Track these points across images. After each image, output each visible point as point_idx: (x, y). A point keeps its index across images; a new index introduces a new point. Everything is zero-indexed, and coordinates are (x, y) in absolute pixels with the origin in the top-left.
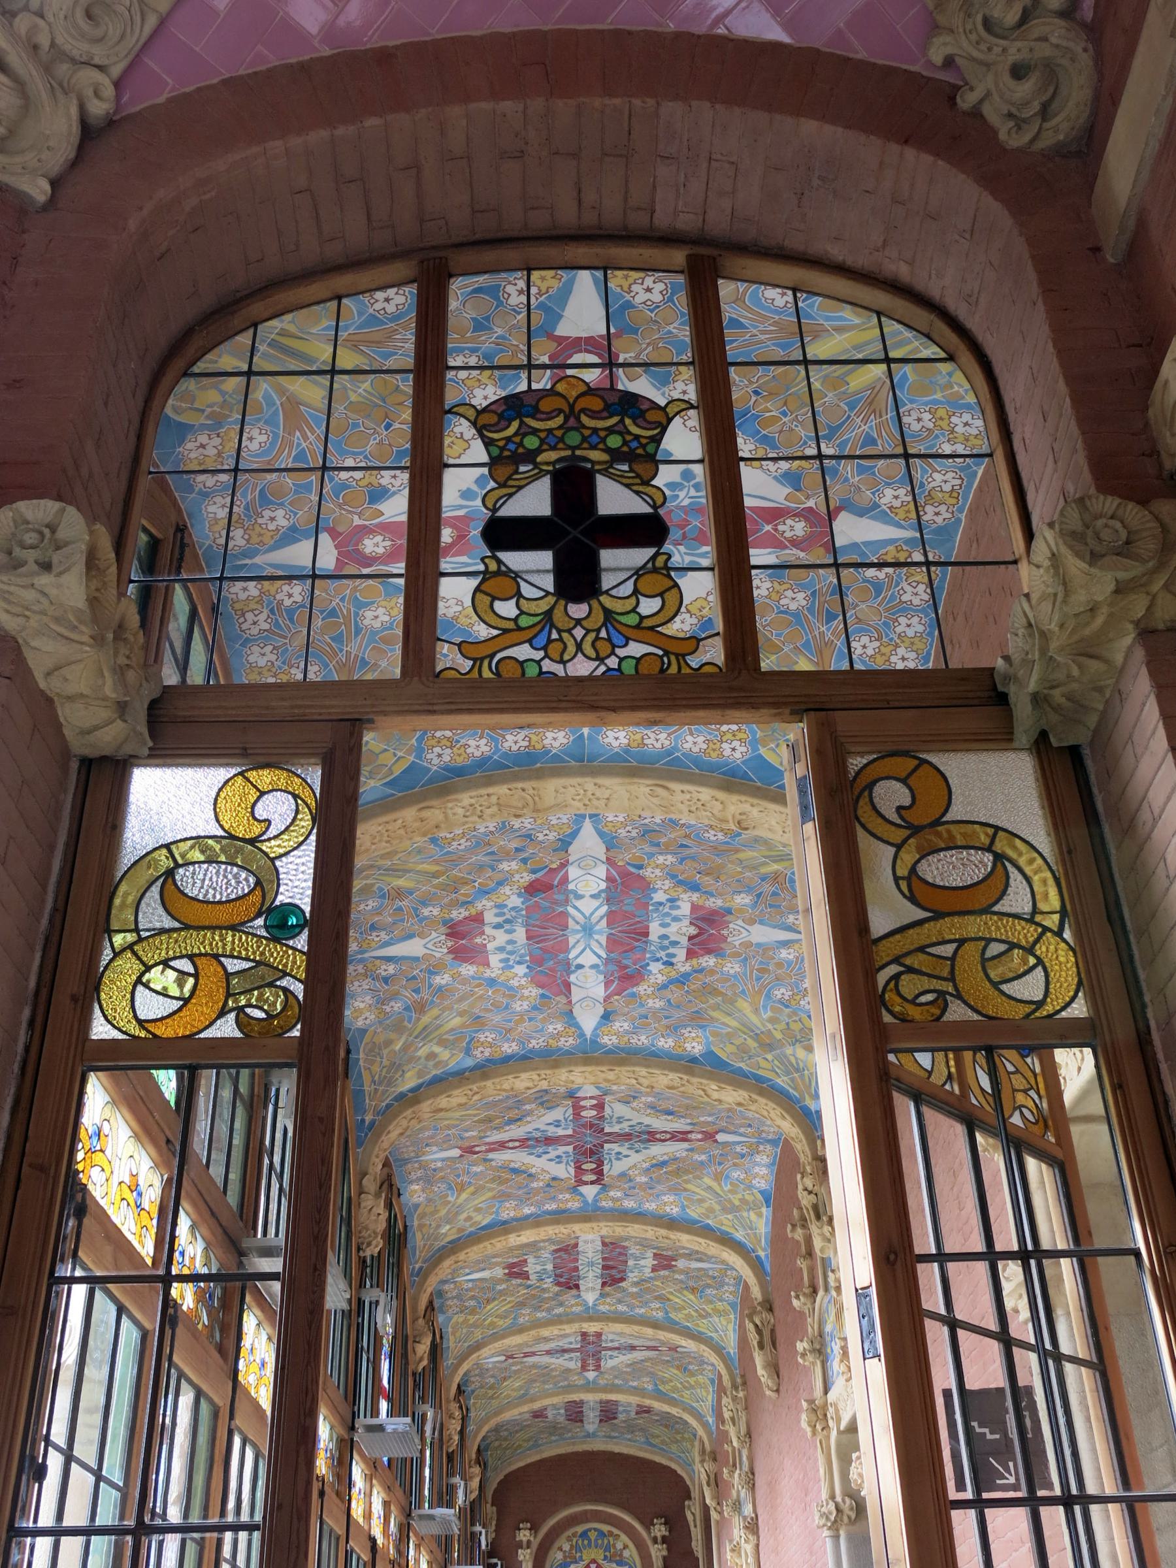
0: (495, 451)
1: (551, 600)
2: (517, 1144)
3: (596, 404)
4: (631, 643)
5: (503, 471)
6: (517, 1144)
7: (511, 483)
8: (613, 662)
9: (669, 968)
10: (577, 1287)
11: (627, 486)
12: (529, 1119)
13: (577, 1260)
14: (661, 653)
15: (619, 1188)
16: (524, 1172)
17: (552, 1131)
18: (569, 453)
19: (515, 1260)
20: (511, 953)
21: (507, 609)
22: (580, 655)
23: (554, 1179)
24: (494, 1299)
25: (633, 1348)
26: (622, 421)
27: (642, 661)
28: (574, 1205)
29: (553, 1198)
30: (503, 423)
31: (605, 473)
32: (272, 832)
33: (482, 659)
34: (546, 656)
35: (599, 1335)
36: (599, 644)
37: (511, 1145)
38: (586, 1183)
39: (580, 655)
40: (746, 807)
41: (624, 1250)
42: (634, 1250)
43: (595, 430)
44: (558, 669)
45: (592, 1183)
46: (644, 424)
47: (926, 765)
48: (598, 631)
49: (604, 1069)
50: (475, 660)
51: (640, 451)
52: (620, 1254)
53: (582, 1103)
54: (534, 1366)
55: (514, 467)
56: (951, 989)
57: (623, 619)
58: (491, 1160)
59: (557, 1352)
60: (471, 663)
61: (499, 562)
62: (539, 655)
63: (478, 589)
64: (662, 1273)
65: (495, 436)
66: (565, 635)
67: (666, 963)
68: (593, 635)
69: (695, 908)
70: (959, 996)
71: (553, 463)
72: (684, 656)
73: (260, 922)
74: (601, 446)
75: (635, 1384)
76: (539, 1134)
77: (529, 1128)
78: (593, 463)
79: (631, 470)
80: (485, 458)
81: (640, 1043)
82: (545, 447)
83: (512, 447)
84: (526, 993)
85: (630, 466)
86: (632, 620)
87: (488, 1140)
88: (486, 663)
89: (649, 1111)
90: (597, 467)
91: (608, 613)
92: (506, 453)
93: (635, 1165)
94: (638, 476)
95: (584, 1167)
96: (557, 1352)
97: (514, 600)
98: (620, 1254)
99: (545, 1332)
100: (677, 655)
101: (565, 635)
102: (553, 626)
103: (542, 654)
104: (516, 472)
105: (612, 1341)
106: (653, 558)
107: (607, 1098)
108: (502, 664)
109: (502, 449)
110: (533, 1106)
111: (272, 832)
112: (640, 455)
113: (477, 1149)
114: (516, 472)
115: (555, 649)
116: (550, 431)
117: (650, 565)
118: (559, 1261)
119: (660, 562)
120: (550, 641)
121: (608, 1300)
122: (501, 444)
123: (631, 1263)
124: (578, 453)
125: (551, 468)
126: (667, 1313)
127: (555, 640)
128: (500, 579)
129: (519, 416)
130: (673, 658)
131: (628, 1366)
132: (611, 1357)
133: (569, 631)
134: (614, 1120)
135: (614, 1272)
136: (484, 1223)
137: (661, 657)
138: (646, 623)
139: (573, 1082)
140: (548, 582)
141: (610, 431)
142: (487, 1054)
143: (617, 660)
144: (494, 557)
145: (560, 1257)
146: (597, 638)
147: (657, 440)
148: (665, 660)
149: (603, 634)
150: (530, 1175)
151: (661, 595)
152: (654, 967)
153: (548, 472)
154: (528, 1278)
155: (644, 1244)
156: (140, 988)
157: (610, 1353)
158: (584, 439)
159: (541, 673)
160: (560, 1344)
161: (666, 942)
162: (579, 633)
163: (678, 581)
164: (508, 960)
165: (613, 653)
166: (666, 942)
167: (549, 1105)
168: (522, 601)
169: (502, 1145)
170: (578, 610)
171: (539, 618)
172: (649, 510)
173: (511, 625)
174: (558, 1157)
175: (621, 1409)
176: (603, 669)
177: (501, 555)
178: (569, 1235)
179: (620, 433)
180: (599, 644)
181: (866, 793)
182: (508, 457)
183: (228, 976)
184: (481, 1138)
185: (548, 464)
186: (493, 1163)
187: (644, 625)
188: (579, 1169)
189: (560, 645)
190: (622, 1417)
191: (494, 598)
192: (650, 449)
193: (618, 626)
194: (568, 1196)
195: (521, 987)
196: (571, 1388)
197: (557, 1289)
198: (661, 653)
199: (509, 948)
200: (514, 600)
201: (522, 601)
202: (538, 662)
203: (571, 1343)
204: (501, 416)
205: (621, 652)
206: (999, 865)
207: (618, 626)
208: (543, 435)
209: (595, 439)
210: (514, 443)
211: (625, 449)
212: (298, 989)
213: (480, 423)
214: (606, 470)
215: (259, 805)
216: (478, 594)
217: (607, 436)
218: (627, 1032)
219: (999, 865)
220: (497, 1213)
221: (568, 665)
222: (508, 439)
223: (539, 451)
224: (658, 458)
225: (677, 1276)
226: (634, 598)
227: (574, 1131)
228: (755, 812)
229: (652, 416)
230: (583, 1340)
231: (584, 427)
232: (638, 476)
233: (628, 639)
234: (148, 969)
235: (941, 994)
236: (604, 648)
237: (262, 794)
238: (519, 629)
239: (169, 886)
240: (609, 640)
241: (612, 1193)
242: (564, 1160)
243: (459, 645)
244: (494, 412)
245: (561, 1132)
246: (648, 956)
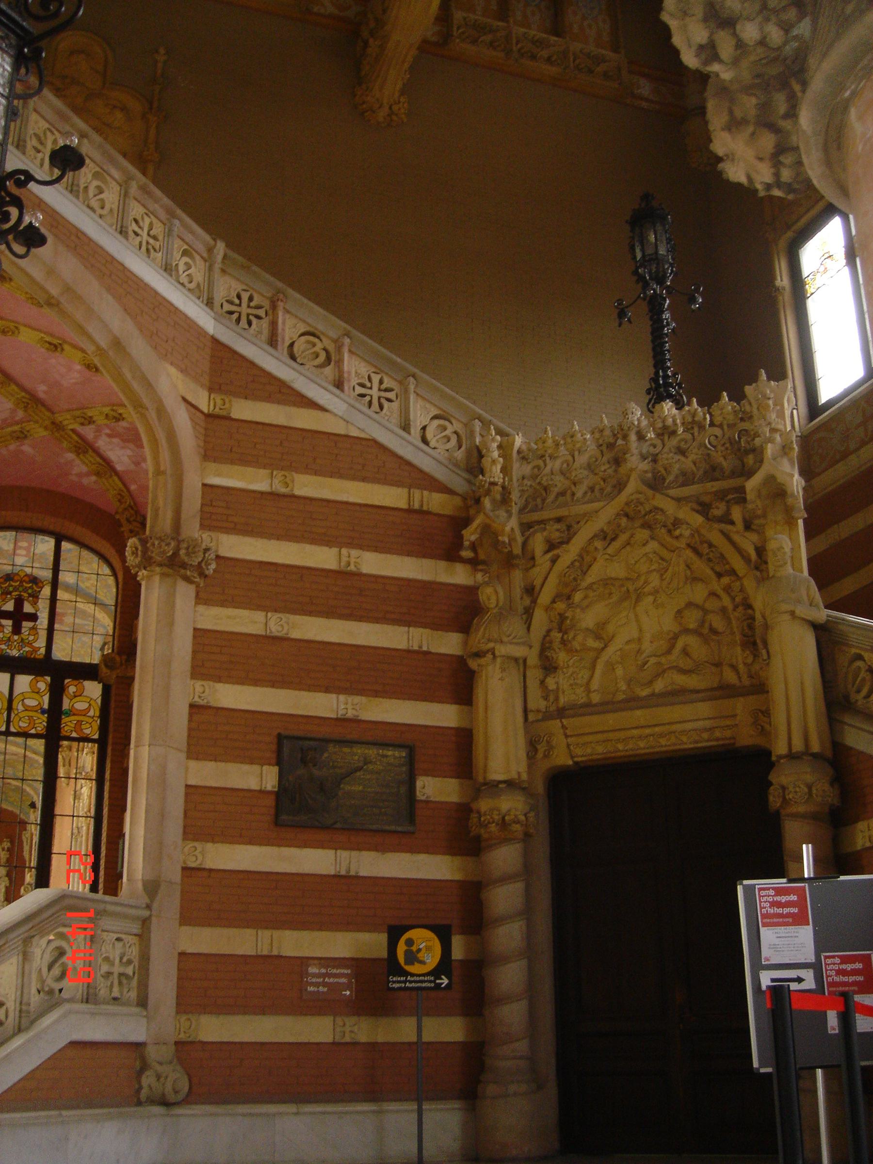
5: (4, 597)
31: (27, 600)
86: (27, 641)
140: (10, 629)
141: (30, 588)
170: (16, 637)
209: (25, 590)
223: (12, 592)
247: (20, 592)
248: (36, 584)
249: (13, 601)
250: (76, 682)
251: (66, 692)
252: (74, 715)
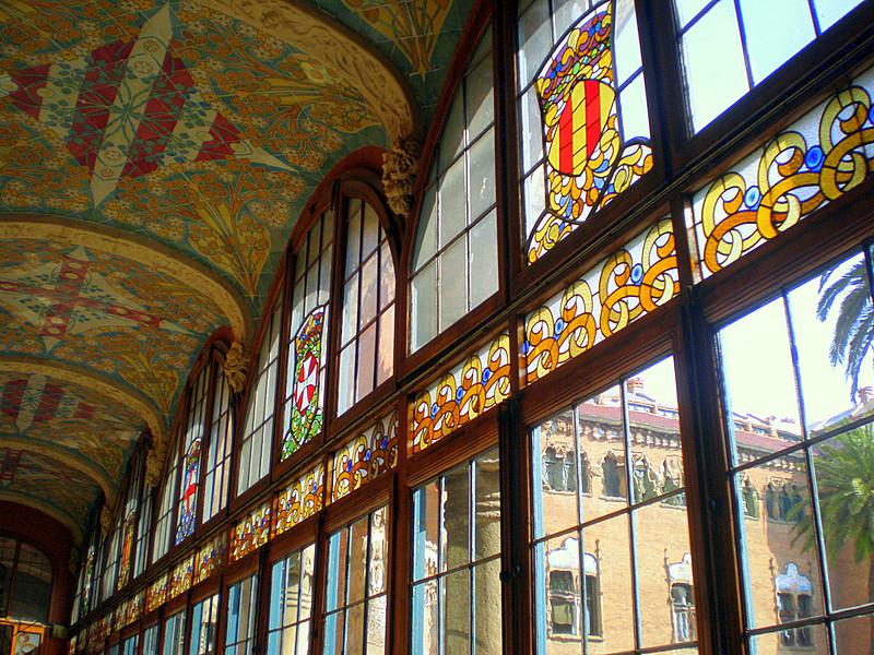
20: (59, 114)
38: (51, 335)
45: (55, 335)
67: (178, 159)
69: (219, 116)
93: (91, 330)
142: (12, 202)
152: (168, 160)
155: (80, 391)
157: (23, 469)
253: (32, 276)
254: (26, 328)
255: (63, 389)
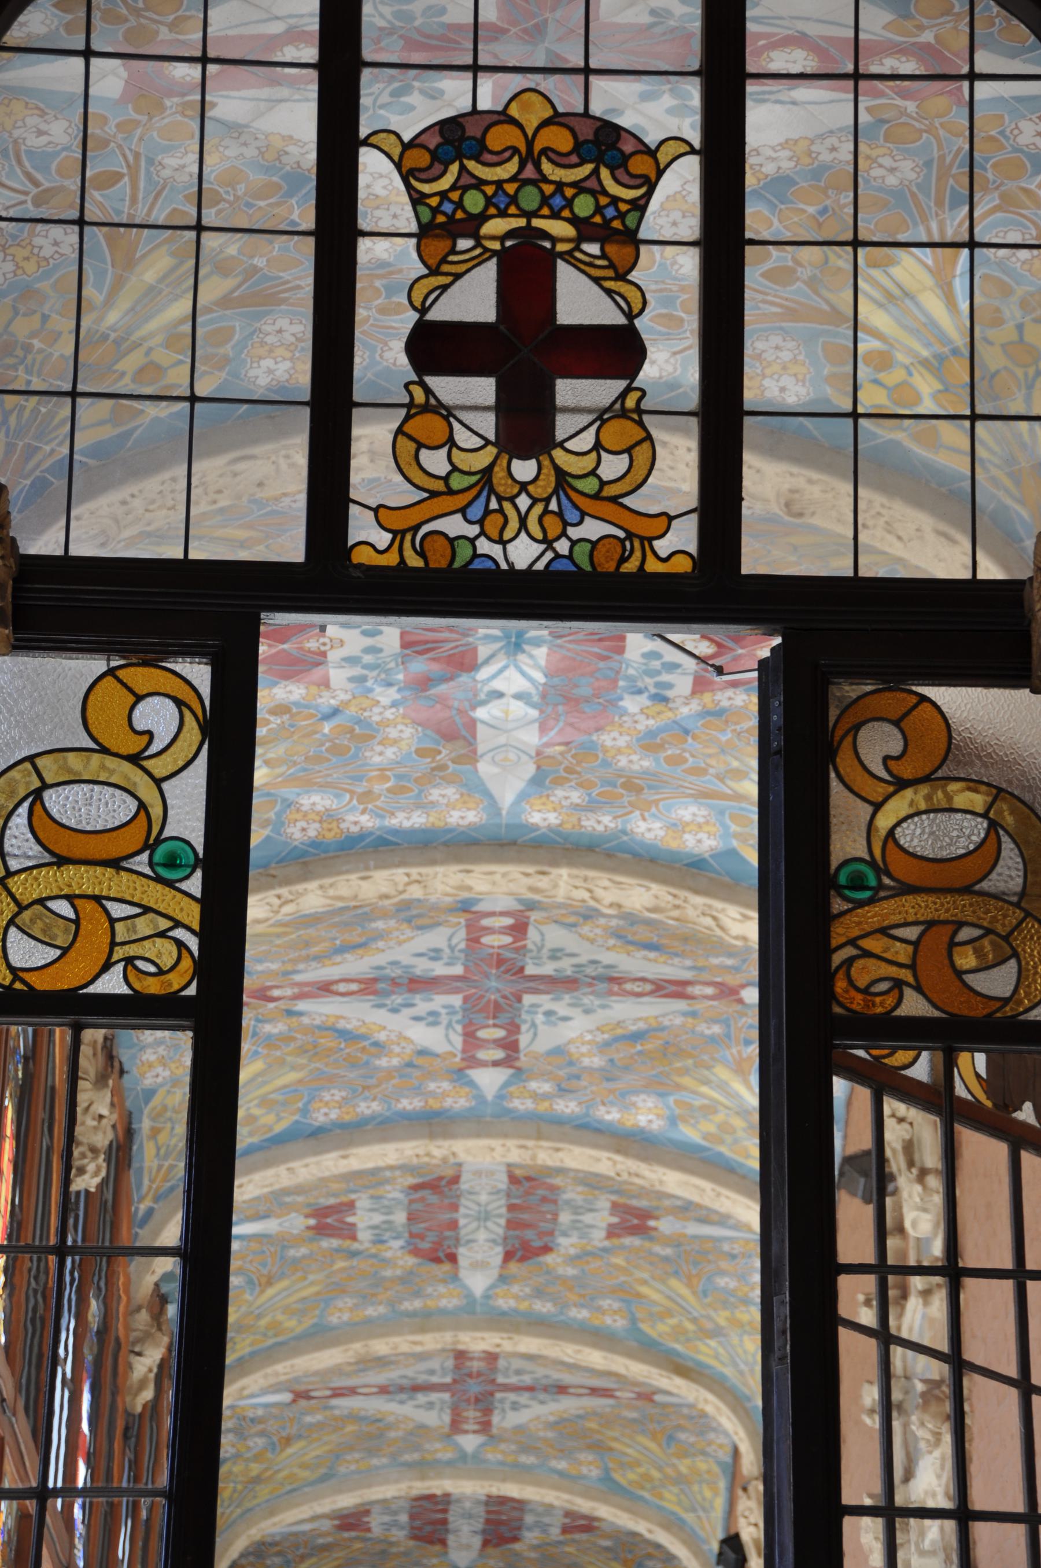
0: (426, 215)
1: (492, 450)
2: (354, 987)
3: (560, 140)
4: (588, 520)
5: (438, 247)
6: (354, 987)
7: (445, 268)
8: (562, 546)
9: (660, 707)
10: (453, 1258)
11: (597, 281)
12: (381, 944)
13: (455, 1207)
14: (621, 534)
15: (543, 1076)
16: (363, 1037)
17: (423, 967)
18: (522, 222)
19: (332, 1201)
21: (436, 462)
22: (523, 535)
23: (423, 1052)
24: (282, 1276)
25: (562, 1389)
26: (596, 172)
27: (599, 546)
28: (459, 1102)
29: (418, 1091)
30: (438, 168)
31: (568, 257)
32: (154, 749)
33: (404, 532)
34: (483, 533)
35: (492, 1358)
36: (548, 520)
37: (342, 987)
38: (483, 1064)
39: (523, 535)
40: (800, 482)
41: (551, 1198)
42: (572, 1194)
43: (560, 186)
44: (495, 551)
45: (496, 1064)
46: (625, 179)
47: (926, 704)
48: (547, 500)
49: (530, 869)
50: (395, 533)
51: (616, 224)
52: (544, 1200)
53: (486, 922)
54: (354, 1417)
55: (448, 243)
56: (911, 979)
57: (579, 484)
58: (301, 1014)
59: (402, 1389)
60: (389, 536)
61: (428, 391)
62: (473, 530)
63: (399, 431)
64: (628, 1241)
65: (426, 188)
66: (507, 506)
68: (539, 509)
70: (918, 989)
71: (502, 239)
72: (650, 540)
73: (145, 856)
74: (566, 213)
75: (562, 1465)
76: (399, 972)
77: (381, 959)
78: (554, 240)
79: (604, 256)
80: (414, 228)
81: (600, 828)
82: (492, 211)
83: (448, 207)
84: (393, 733)
85: (602, 249)
86: (589, 486)
87: (298, 978)
88: (408, 537)
89: (612, 942)
90: (561, 247)
91: (562, 476)
92: (441, 219)
94: (612, 266)
95: (482, 1034)
96: (402, 1389)
97: (446, 449)
98: (544, 1200)
99: (381, 1347)
100: (642, 539)
101: (507, 506)
102: (492, 491)
103: (475, 530)
104: (453, 251)
105: (518, 1372)
106: (623, 396)
107: (534, 916)
108: (429, 539)
109: (435, 211)
110: (392, 923)
111: (154, 749)
112: (616, 231)
113: (276, 993)
114: (453, 251)
115: (493, 524)
116: (499, 184)
117: (618, 406)
118: (415, 1206)
119: (630, 403)
120: (487, 512)
121: (515, 1289)
122: (434, 202)
123: (565, 1218)
124: (536, 223)
125: (496, 246)
126: (634, 1321)
127: (495, 511)
128: (429, 417)
129: (460, 156)
130: (637, 544)
131: (553, 1426)
132: (515, 1407)
133: (512, 499)
134: (545, 952)
135: (529, 1234)
136: (278, 1128)
137: (622, 541)
138: (609, 491)
139: (469, 889)
140: (487, 424)
141: (579, 186)
142: (312, 833)
143: (569, 544)
144: (422, 384)
145: (422, 1199)
146: (546, 511)
147: (640, 206)
148: (628, 544)
149: (553, 506)
150: (376, 1044)
151: (629, 450)
152: (631, 704)
153: (494, 253)
154: (354, 1238)
155: (593, 1182)
156: (13, 931)
157: (512, 1396)
158: (545, 200)
159: (475, 556)
160: (410, 1372)
161: (656, 664)
162: (523, 502)
163: (654, 433)
164: (362, 679)
165: (564, 534)
166: (656, 664)
167: (420, 922)
168: (454, 450)
169: (326, 988)
170: (524, 469)
171: (474, 479)
172: (622, 320)
173: (439, 486)
174: (432, 1013)
175: (529, 1519)
176: (549, 555)
177: (431, 381)
178: (445, 1160)
179: (593, 193)
180: (548, 520)
181: (849, 739)
182: (441, 225)
183: (112, 921)
184: (286, 973)
185: (493, 238)
186: (305, 1020)
187: (604, 494)
188: (470, 1036)
189: (499, 519)
190: (531, 1537)
191: (420, 445)
192: (631, 220)
193: (572, 494)
194: (446, 1085)
195: (386, 723)
196: (424, 1467)
197: (411, 1261)
198: (621, 534)
199: (368, 659)
200: (446, 449)
201: (454, 450)
202: (472, 541)
203: (432, 1372)
204: (434, 155)
205: (574, 533)
206: (993, 835)
207: (572, 494)
208: (490, 190)
210: (451, 201)
211: (598, 219)
212: (193, 943)
213: (407, 164)
214: (570, 253)
215: (137, 713)
216: (400, 437)
217: (575, 196)
218: (576, 807)
219: (993, 835)
220: (305, 1111)
221: (509, 547)
222: (443, 195)
223: (483, 218)
224: (642, 235)
225: (658, 1249)
226: (594, 454)
227: (467, 968)
228: (815, 492)
229: (640, 165)
230: (457, 1367)
231: (545, 180)
232: (612, 266)
233: (583, 514)
234: (21, 908)
235: (898, 984)
236: (553, 526)
237: (139, 698)
238: (451, 492)
239: (38, 807)
240: (560, 514)
241: (533, 1085)
242: (444, 1019)
243: (376, 510)
244: (423, 146)
245: (440, 969)
246: (621, 683)
247: (529, 215)
248: (619, 164)
249: (490, 270)
250: (893, 702)
251: (844, 760)
252: (907, 889)
253: (398, 958)
254: (419, 1061)
255: (557, 1181)
